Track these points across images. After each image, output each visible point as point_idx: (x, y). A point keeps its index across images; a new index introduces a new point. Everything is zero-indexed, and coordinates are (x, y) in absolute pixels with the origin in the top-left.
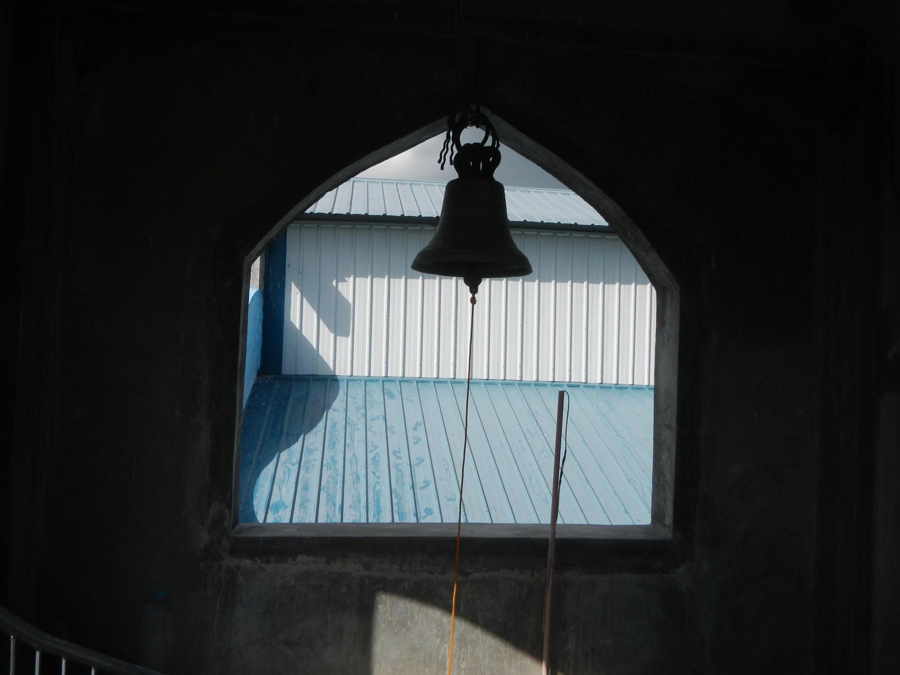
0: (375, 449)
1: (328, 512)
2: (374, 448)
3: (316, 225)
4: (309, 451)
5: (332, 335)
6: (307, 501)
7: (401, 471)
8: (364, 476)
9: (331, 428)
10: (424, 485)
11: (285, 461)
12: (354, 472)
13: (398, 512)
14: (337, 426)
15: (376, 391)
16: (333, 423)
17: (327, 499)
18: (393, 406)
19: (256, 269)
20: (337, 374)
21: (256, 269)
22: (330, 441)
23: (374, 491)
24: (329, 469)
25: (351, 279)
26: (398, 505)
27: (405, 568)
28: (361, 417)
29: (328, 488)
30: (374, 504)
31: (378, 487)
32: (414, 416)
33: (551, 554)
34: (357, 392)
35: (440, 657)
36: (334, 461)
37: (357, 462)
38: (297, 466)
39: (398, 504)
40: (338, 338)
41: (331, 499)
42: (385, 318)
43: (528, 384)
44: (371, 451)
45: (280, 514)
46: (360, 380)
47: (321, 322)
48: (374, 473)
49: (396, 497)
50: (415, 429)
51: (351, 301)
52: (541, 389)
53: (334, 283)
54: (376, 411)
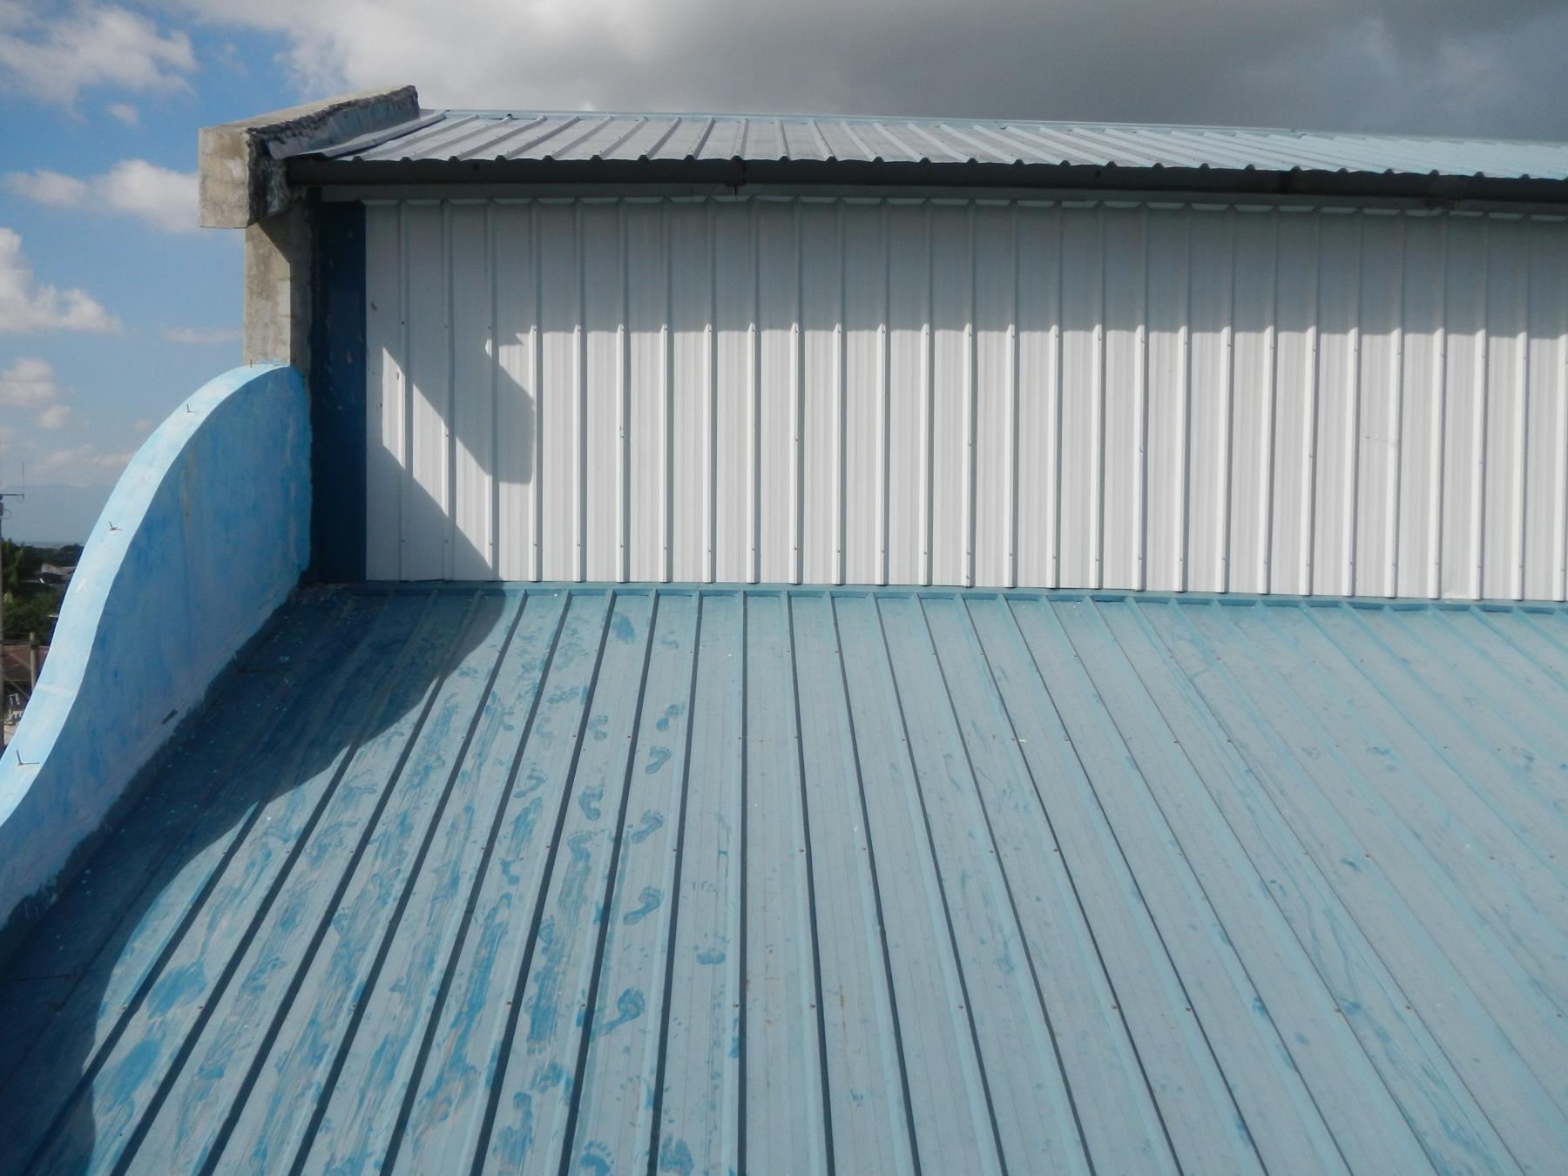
0: (534, 788)
1: (318, 1006)
2: (534, 782)
3: (438, 202)
4: (350, 795)
5: (487, 480)
6: (274, 966)
7: (588, 855)
8: (470, 879)
9: (436, 725)
10: (640, 906)
11: (271, 826)
12: (450, 862)
13: (537, 1006)
14: (454, 716)
15: (588, 620)
16: (447, 709)
17: (337, 957)
18: (624, 657)
19: (283, 316)
20: (504, 575)
21: (283, 316)
22: (417, 764)
23: (487, 928)
24: (381, 852)
25: (530, 338)
26: (544, 979)
28: (527, 692)
29: (354, 916)
30: (471, 976)
32: (668, 686)
34: (539, 622)
36: (405, 826)
37: (470, 827)
38: (292, 844)
39: (547, 973)
40: (504, 487)
41: (347, 953)
42: (618, 433)
43: (989, 596)
44: (519, 795)
45: (170, 1014)
46: (559, 591)
47: (460, 446)
48: (505, 865)
49: (545, 950)
50: (662, 725)
51: (531, 391)
52: (1023, 609)
53: (488, 347)
54: (571, 675)
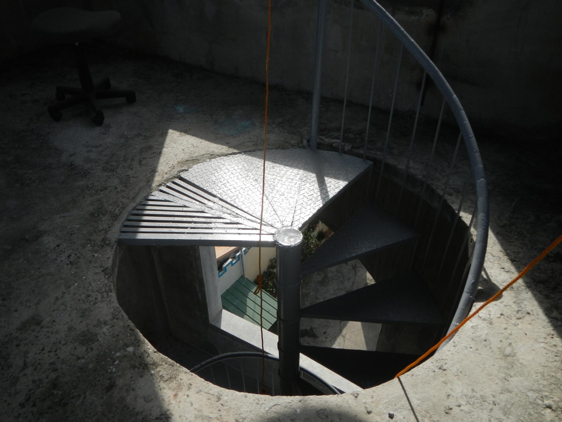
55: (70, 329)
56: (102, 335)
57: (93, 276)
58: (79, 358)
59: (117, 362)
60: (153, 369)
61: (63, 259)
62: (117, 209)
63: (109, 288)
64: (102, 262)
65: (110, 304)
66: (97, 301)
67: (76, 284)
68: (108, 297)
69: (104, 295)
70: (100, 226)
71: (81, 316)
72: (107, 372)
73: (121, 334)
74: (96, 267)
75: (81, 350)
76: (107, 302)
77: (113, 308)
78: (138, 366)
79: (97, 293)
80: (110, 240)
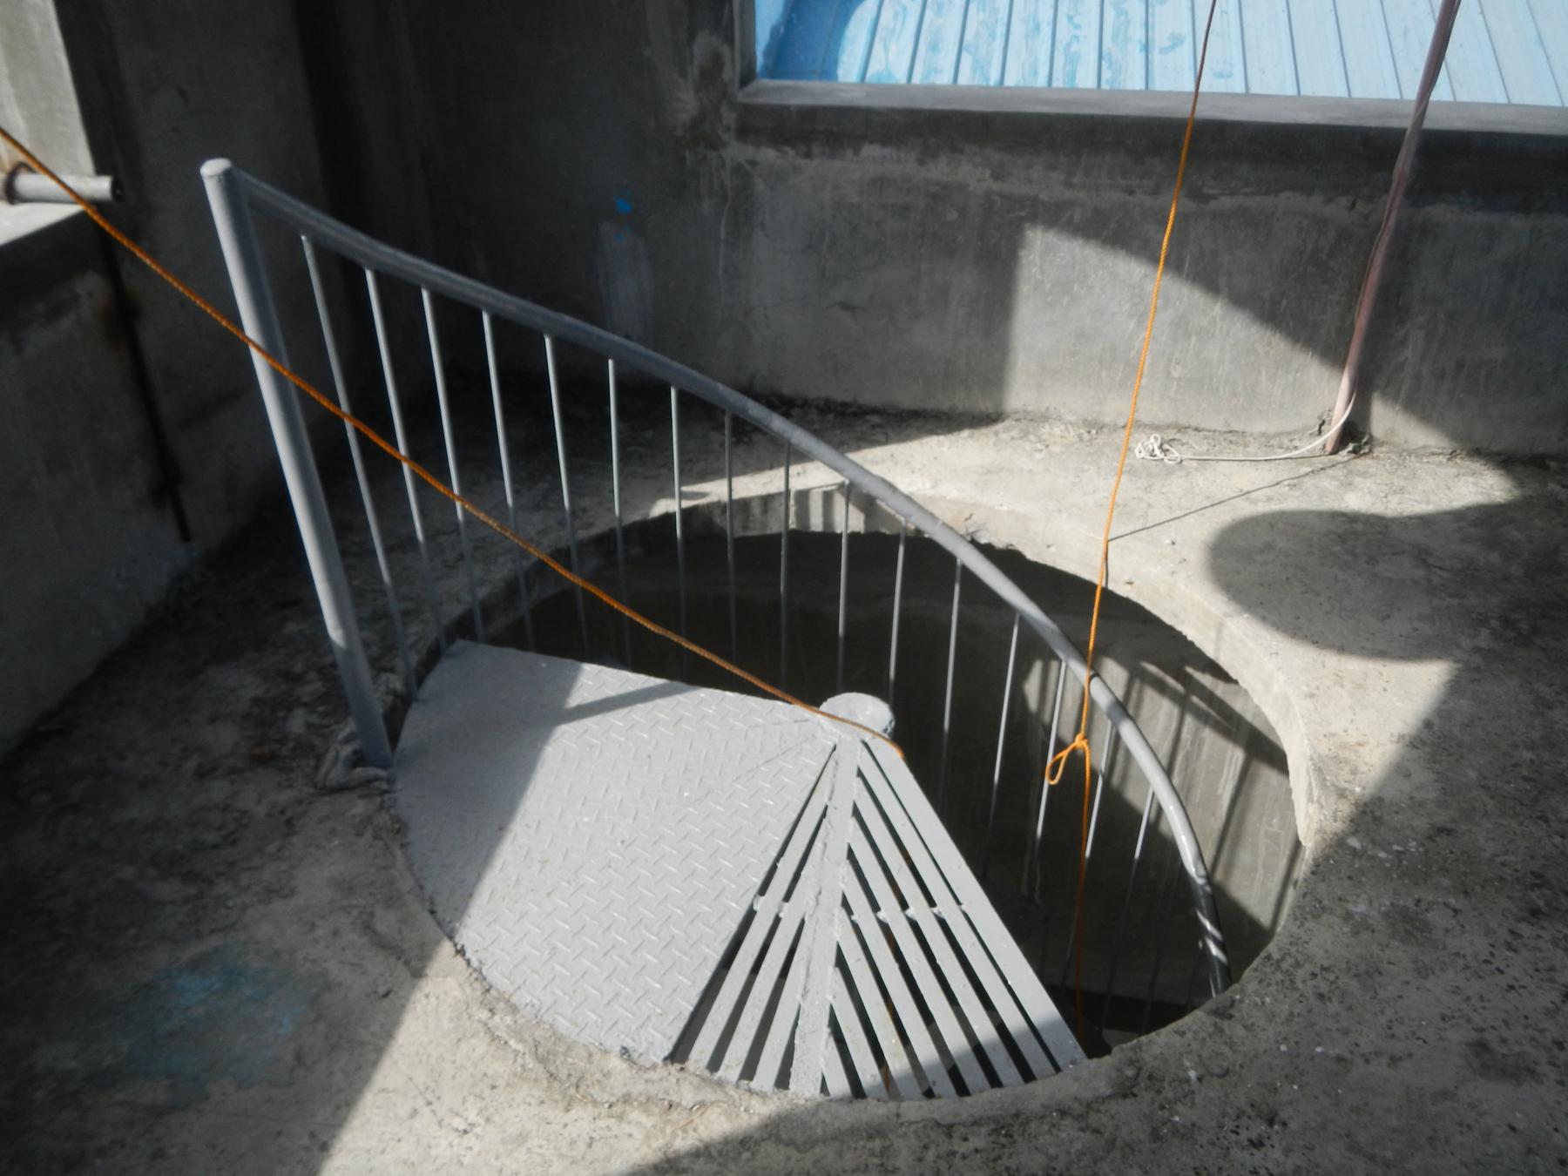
7: (1126, 14)
10: (1169, 44)
27: (1075, 180)
31: (1074, 47)
33: (1404, 163)
35: (1133, 353)
48: (1070, 18)
49: (1109, 68)
55: (1423, 972)
56: (1376, 904)
57: (1264, 1030)
58: (1455, 911)
59: (1396, 847)
60: (1353, 792)
61: (1277, 1154)
62: (962, 1148)
63: (1265, 967)
64: (1204, 1039)
65: (1301, 938)
66: (1317, 971)
67: (1319, 1049)
68: (1289, 954)
69: (1291, 966)
70: (1078, 1145)
71: (1380, 973)
72: (1427, 852)
73: (1342, 875)
74: (1231, 1044)
75: (1437, 918)
76: (1300, 949)
77: (1302, 924)
78: (1370, 815)
79: (1299, 985)
80: (1119, 1070)
